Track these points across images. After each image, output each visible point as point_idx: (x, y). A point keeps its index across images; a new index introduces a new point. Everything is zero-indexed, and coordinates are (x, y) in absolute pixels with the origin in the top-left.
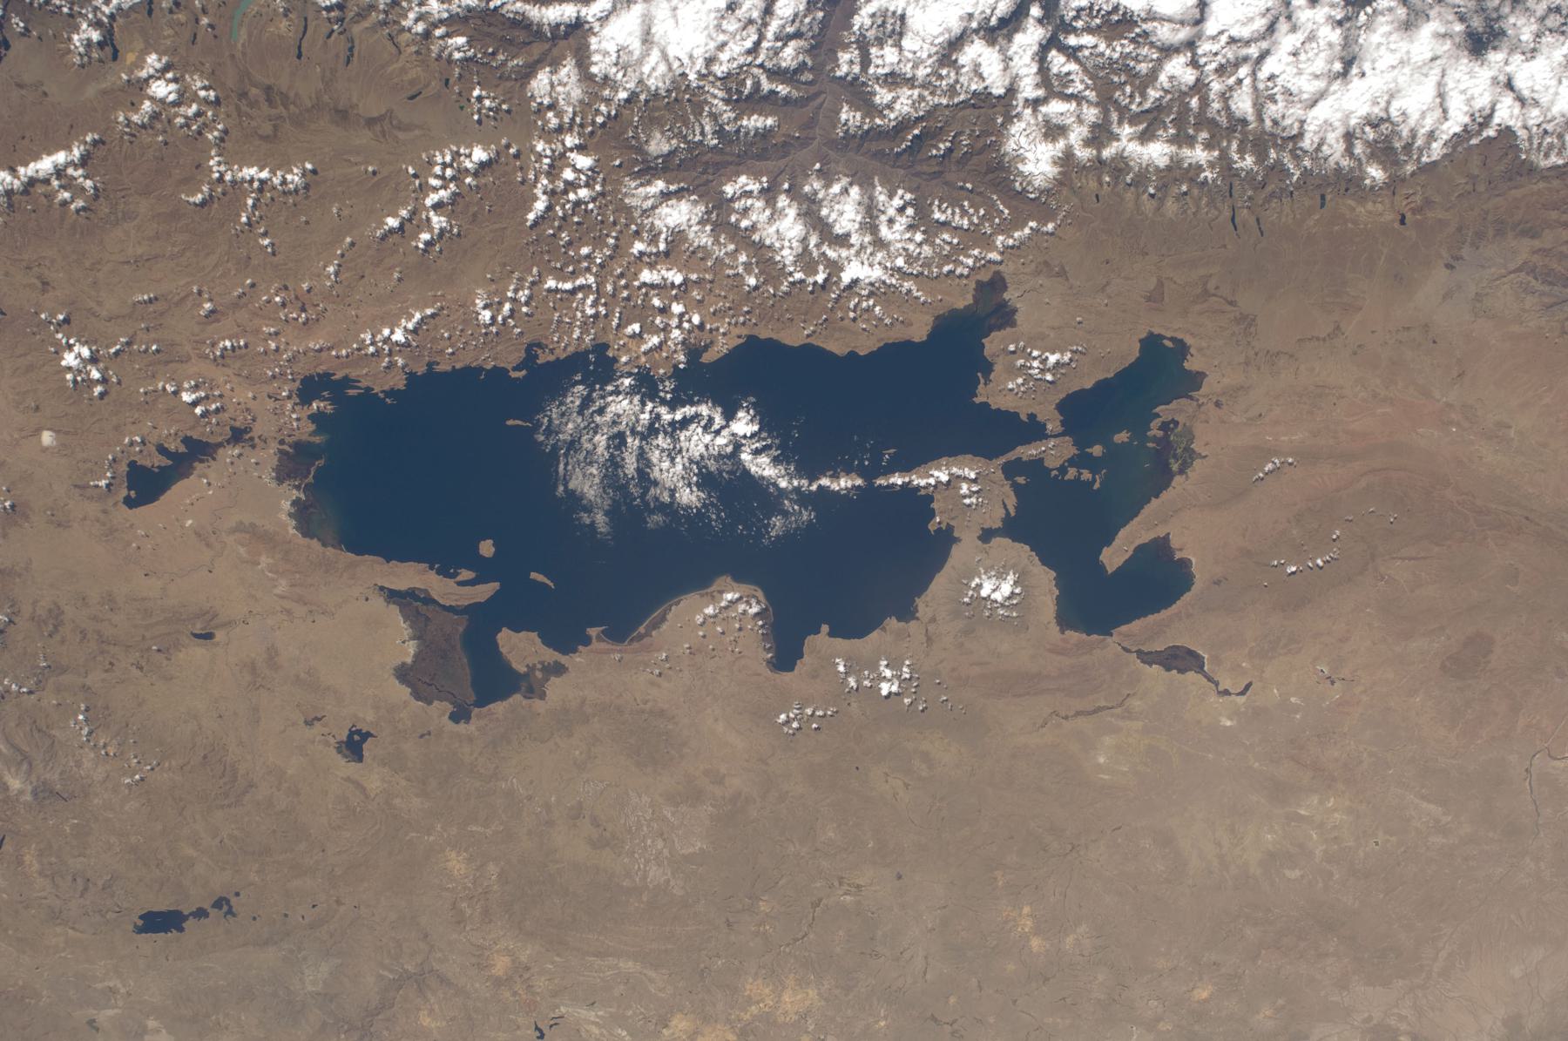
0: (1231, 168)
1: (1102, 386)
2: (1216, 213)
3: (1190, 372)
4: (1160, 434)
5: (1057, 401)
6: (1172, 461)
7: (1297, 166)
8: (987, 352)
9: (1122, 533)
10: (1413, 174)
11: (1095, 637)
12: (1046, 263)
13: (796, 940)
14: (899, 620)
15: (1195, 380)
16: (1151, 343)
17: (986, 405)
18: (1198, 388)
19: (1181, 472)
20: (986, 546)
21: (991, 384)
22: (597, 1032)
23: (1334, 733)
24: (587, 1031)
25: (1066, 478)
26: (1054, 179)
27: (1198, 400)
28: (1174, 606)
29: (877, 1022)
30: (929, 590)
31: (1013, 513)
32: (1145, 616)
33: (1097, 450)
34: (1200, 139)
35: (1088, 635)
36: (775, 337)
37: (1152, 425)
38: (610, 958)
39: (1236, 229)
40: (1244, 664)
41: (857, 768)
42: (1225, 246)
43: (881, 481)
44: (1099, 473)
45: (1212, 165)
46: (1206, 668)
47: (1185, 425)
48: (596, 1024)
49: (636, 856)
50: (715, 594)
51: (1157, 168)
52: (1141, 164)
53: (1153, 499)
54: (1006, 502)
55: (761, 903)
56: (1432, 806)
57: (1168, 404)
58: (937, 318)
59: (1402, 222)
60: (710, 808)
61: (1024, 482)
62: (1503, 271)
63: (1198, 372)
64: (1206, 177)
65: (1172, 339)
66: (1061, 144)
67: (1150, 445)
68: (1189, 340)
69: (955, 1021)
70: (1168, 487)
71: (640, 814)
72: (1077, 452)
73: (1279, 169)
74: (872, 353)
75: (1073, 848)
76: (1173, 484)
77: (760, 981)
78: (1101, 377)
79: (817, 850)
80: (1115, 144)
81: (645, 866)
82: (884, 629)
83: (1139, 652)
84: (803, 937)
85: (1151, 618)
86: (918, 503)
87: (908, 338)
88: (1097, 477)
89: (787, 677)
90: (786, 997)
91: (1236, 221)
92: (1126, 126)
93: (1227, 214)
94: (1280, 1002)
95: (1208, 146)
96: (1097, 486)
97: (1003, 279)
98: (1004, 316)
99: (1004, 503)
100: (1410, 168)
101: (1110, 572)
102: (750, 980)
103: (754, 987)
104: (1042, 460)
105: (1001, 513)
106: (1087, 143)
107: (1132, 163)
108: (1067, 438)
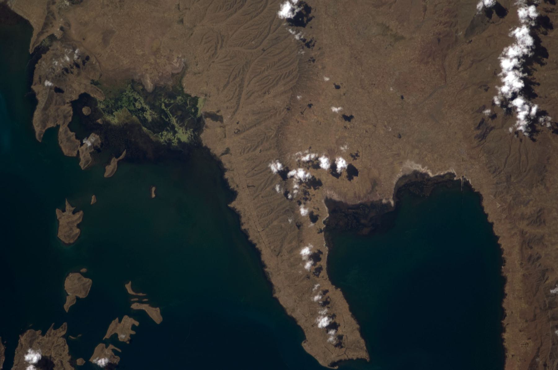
6: (165, 137)
27: (52, 38)
28: (503, 243)
32: (502, 314)
37: (66, 151)
44: (128, 299)
47: (94, 83)
67: (110, 169)
70: (219, 163)
72: (62, 332)
76: (217, 150)
88: (135, 306)
101: (363, 354)
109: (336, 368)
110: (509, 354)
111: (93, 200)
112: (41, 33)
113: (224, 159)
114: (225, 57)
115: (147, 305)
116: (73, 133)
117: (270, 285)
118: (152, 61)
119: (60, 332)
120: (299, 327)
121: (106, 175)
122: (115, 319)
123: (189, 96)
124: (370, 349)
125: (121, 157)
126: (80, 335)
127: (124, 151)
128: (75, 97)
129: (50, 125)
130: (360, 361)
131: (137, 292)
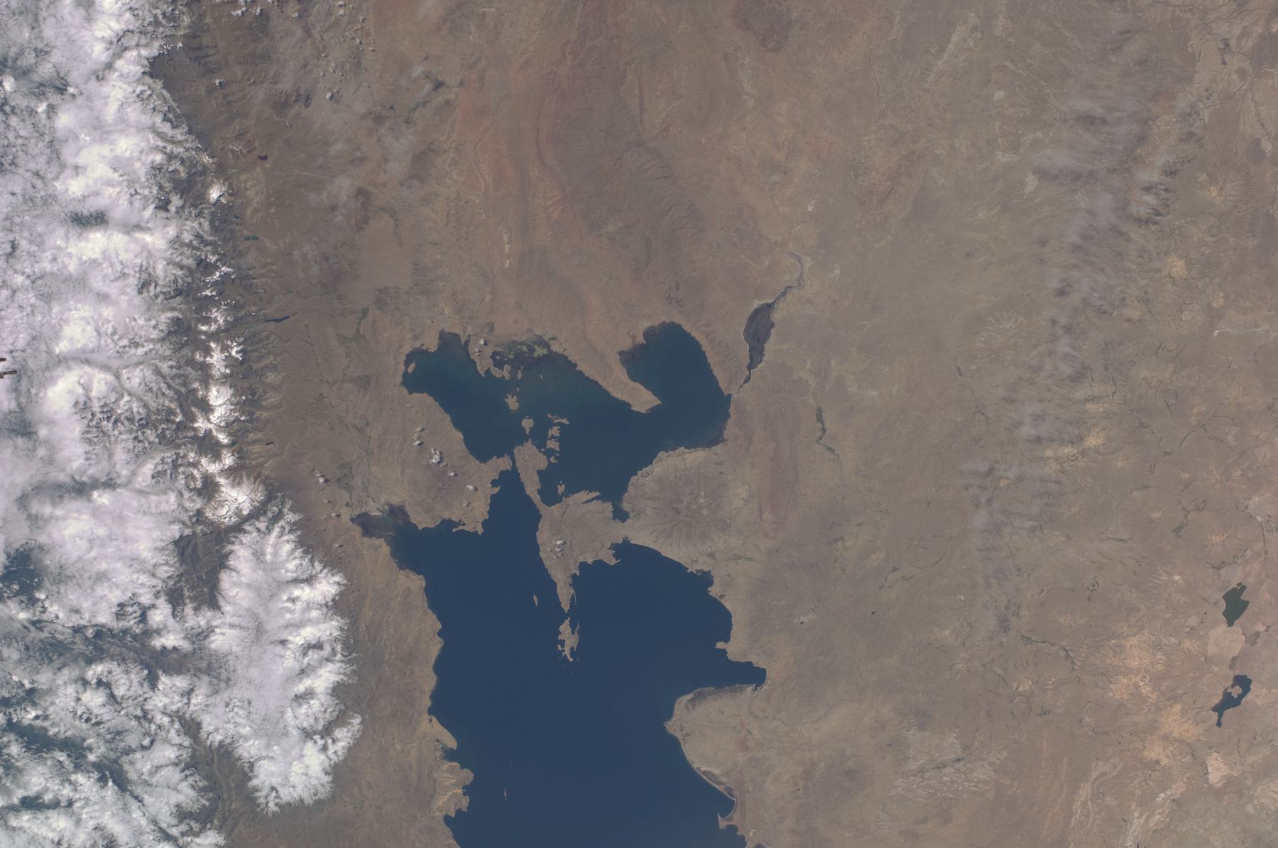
0: (227, 330)
1: (457, 424)
2: (273, 338)
3: (440, 347)
4: (507, 367)
5: (477, 462)
6: (536, 355)
7: (217, 268)
8: (431, 525)
10: (212, 156)
11: (732, 411)
12: (339, 481)
13: (1068, 657)
14: (711, 583)
15: (449, 341)
16: (412, 383)
17: (484, 523)
18: (456, 336)
19: (547, 345)
20: (632, 515)
21: (463, 519)
22: (1157, 817)
23: (854, 160)
24: (1156, 824)
25: (558, 449)
26: (254, 483)
27: (469, 336)
29: (1175, 582)
30: (679, 561)
31: (597, 494)
32: (709, 365)
33: (527, 424)
34: (202, 359)
35: (730, 417)
36: (429, 694)
37: (498, 376)
38: (1074, 807)
39: (288, 317)
40: (767, 263)
41: (873, 613)
42: (306, 326)
43: (566, 605)
45: (225, 348)
46: (770, 301)
48: (1148, 818)
49: (961, 788)
50: (684, 733)
51: (234, 395)
52: (231, 410)
54: (586, 500)
55: (1021, 689)
56: (955, 38)
57: (475, 362)
58: (401, 568)
59: (265, 158)
60: (912, 732)
61: (563, 486)
62: (308, 42)
63: (440, 338)
64: (237, 352)
65: (407, 364)
66: (222, 481)
67: (519, 376)
68: (407, 349)
69: (1184, 509)
70: (564, 355)
71: (915, 786)
73: (220, 286)
74: (439, 618)
75: (979, 411)
77: (1113, 687)
79: (964, 644)
80: (215, 433)
81: (974, 782)
82: (722, 596)
83: (750, 367)
84: (1065, 650)
85: (712, 359)
86: (589, 576)
87: (422, 591)
88: (556, 421)
89: (770, 674)
90: (1134, 663)
91: (278, 316)
92: (196, 425)
93: (273, 325)
94: (1203, 177)
95: (208, 351)
96: (565, 421)
97: (360, 516)
98: (397, 512)
99: (587, 502)
100: (206, 159)
101: (659, 402)
102: (1111, 694)
103: (1119, 690)
104: (540, 473)
105: (597, 505)
106: (217, 457)
107: (232, 419)
108: (515, 451)
110: (718, 378)
111: (518, 390)
113: (565, 353)
117: (608, 393)
124: (661, 400)
128: (491, 354)
129: (486, 369)
130: (658, 405)
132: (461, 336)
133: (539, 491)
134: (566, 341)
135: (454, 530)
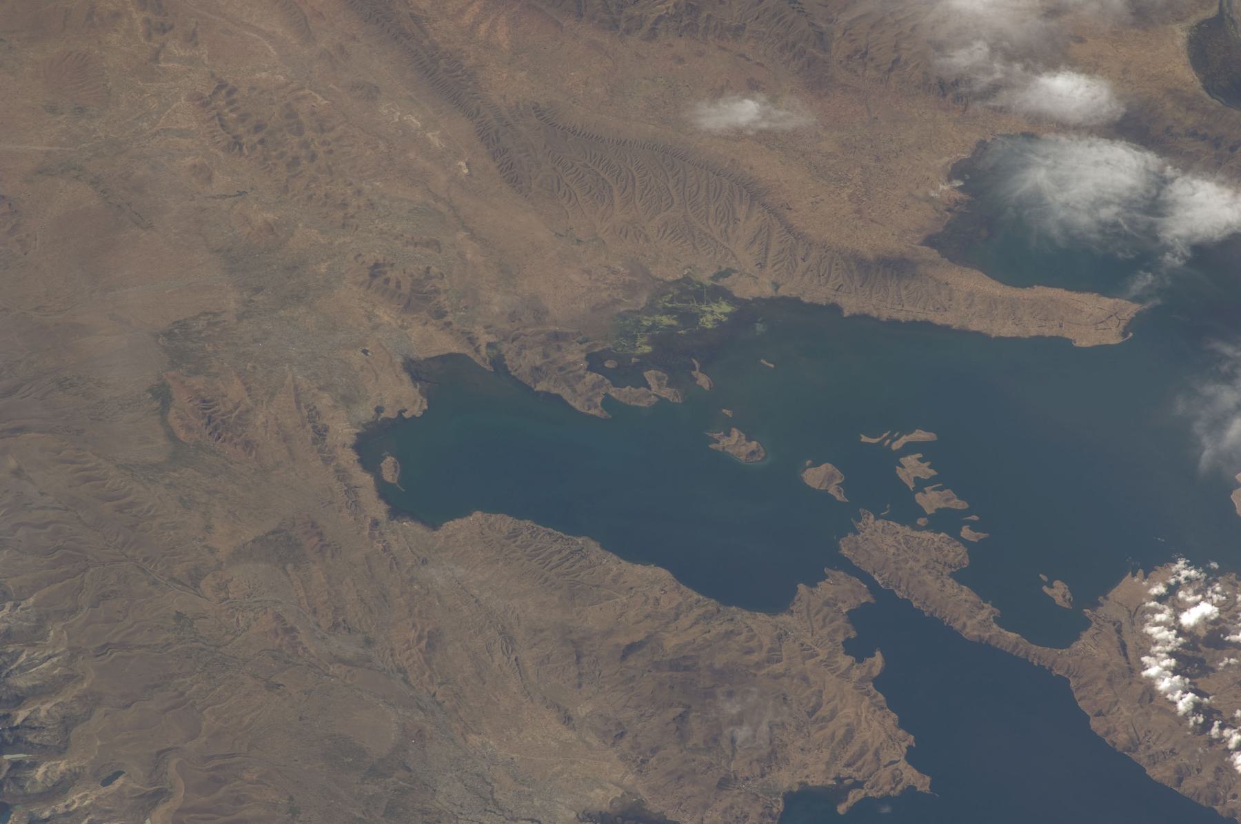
9: (1006, 329)
17: (913, 757)
19: (718, 293)
53: (846, 314)
57: (558, 398)
61: (1057, 583)
78: (612, 564)
96: (921, 435)
104: (960, 576)
108: (845, 551)
109: (1131, 334)
112: (477, 350)
113: (783, 292)
114: (659, 231)
115: (904, 437)
116: (627, 388)
118: (603, 286)
119: (868, 519)
120: (1051, 337)
121: (707, 387)
122: (896, 469)
123: (678, 281)
125: (697, 366)
126: (888, 506)
127: (691, 360)
128: (584, 364)
131: (880, 437)
132: (469, 352)
133: (1001, 622)
134: (761, 265)
135: (842, 809)
